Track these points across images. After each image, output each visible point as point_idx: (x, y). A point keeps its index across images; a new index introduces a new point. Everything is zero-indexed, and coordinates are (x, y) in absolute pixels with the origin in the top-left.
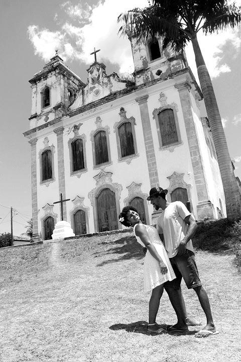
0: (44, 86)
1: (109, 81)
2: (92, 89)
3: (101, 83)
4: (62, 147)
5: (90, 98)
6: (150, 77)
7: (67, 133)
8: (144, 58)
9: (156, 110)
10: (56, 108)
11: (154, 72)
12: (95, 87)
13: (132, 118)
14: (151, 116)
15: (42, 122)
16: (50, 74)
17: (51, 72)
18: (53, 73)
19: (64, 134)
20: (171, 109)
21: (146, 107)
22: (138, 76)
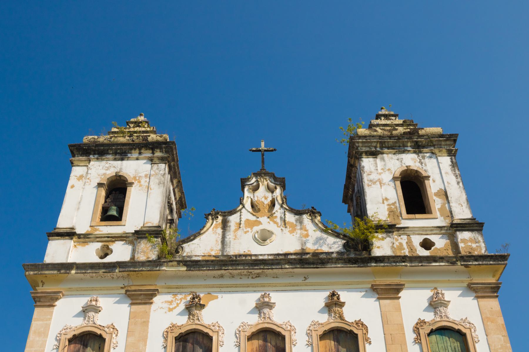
0: (111, 172)
1: (301, 222)
2: (250, 224)
3: (278, 220)
4: (144, 339)
5: (242, 244)
6: (405, 246)
7: (166, 305)
8: (391, 202)
9: (421, 323)
10: (140, 235)
11: (417, 240)
12: (260, 223)
13: (359, 323)
14: (410, 336)
15: (89, 254)
16: (135, 154)
17: (140, 149)
18: (148, 154)
19: (153, 307)
20: (459, 332)
21: (398, 309)
22: (380, 236)
